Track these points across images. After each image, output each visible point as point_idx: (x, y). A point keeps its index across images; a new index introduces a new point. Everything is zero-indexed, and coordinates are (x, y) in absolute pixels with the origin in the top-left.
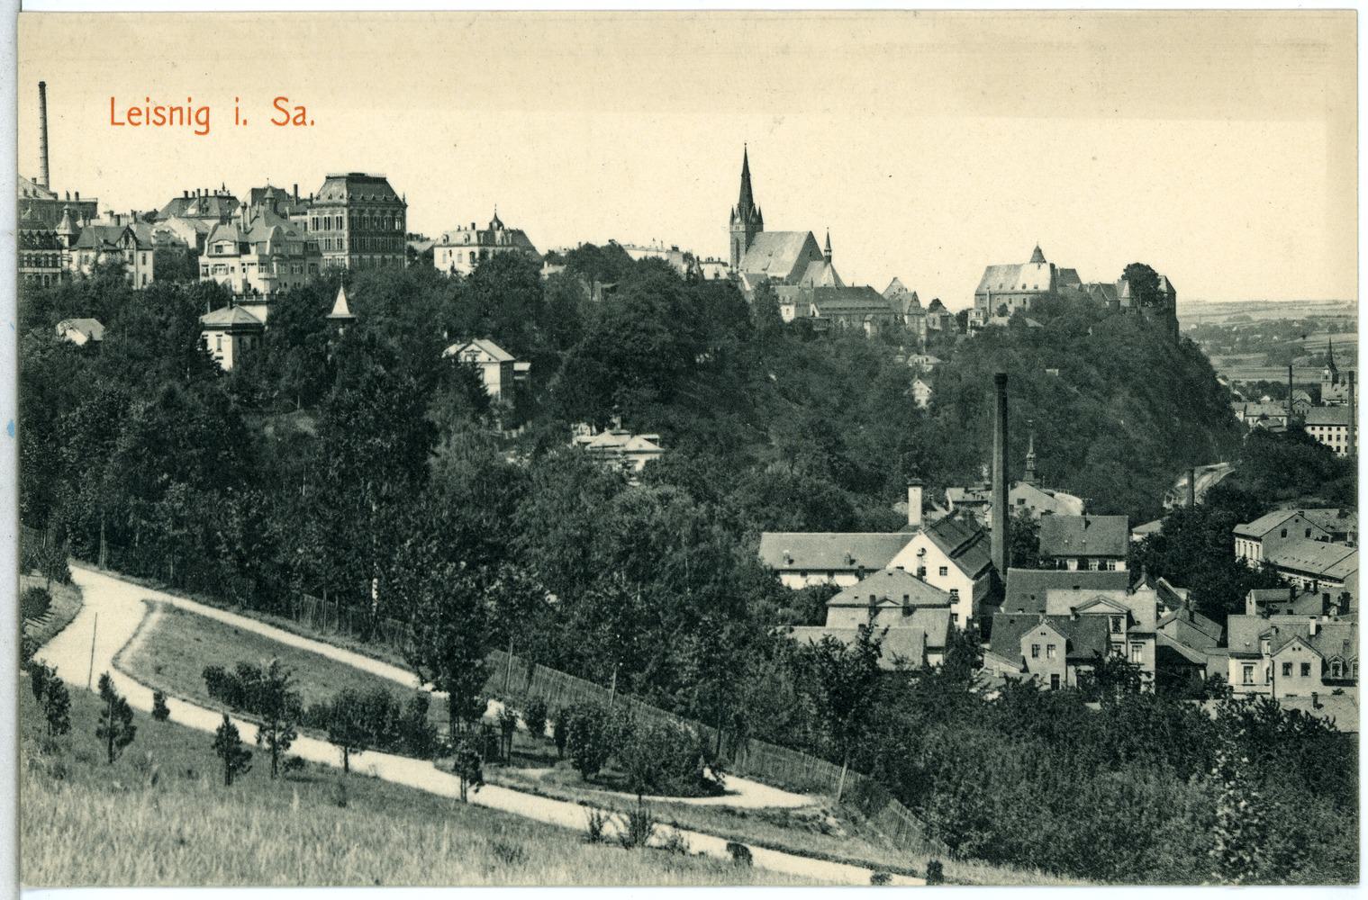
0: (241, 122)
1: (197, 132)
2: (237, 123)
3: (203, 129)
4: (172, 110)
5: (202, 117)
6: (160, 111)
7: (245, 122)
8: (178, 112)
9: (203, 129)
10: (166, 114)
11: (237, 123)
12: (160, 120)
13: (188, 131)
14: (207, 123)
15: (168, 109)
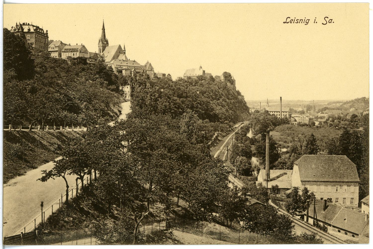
0: (315, 22)
1: (305, 24)
2: (314, 23)
3: (307, 24)
4: (300, 20)
5: (307, 22)
6: (298, 20)
7: (316, 22)
8: (302, 20)
9: (307, 24)
10: (299, 21)
11: (314, 23)
12: (297, 22)
13: (303, 24)
14: (308, 22)
15: (299, 20)
